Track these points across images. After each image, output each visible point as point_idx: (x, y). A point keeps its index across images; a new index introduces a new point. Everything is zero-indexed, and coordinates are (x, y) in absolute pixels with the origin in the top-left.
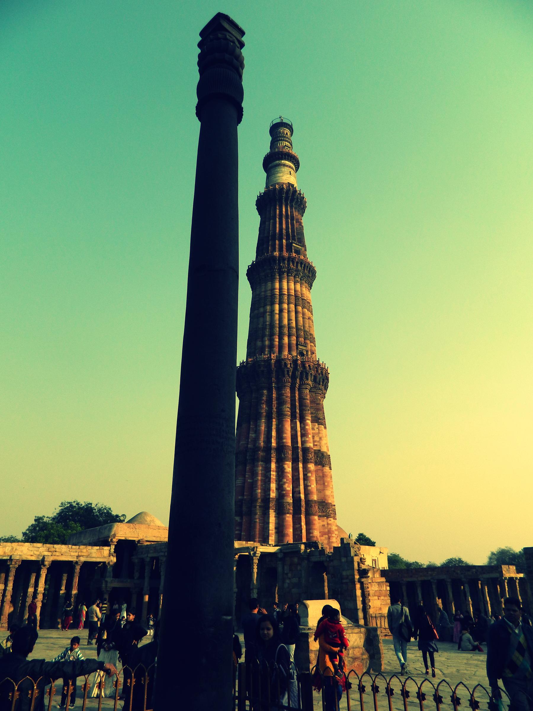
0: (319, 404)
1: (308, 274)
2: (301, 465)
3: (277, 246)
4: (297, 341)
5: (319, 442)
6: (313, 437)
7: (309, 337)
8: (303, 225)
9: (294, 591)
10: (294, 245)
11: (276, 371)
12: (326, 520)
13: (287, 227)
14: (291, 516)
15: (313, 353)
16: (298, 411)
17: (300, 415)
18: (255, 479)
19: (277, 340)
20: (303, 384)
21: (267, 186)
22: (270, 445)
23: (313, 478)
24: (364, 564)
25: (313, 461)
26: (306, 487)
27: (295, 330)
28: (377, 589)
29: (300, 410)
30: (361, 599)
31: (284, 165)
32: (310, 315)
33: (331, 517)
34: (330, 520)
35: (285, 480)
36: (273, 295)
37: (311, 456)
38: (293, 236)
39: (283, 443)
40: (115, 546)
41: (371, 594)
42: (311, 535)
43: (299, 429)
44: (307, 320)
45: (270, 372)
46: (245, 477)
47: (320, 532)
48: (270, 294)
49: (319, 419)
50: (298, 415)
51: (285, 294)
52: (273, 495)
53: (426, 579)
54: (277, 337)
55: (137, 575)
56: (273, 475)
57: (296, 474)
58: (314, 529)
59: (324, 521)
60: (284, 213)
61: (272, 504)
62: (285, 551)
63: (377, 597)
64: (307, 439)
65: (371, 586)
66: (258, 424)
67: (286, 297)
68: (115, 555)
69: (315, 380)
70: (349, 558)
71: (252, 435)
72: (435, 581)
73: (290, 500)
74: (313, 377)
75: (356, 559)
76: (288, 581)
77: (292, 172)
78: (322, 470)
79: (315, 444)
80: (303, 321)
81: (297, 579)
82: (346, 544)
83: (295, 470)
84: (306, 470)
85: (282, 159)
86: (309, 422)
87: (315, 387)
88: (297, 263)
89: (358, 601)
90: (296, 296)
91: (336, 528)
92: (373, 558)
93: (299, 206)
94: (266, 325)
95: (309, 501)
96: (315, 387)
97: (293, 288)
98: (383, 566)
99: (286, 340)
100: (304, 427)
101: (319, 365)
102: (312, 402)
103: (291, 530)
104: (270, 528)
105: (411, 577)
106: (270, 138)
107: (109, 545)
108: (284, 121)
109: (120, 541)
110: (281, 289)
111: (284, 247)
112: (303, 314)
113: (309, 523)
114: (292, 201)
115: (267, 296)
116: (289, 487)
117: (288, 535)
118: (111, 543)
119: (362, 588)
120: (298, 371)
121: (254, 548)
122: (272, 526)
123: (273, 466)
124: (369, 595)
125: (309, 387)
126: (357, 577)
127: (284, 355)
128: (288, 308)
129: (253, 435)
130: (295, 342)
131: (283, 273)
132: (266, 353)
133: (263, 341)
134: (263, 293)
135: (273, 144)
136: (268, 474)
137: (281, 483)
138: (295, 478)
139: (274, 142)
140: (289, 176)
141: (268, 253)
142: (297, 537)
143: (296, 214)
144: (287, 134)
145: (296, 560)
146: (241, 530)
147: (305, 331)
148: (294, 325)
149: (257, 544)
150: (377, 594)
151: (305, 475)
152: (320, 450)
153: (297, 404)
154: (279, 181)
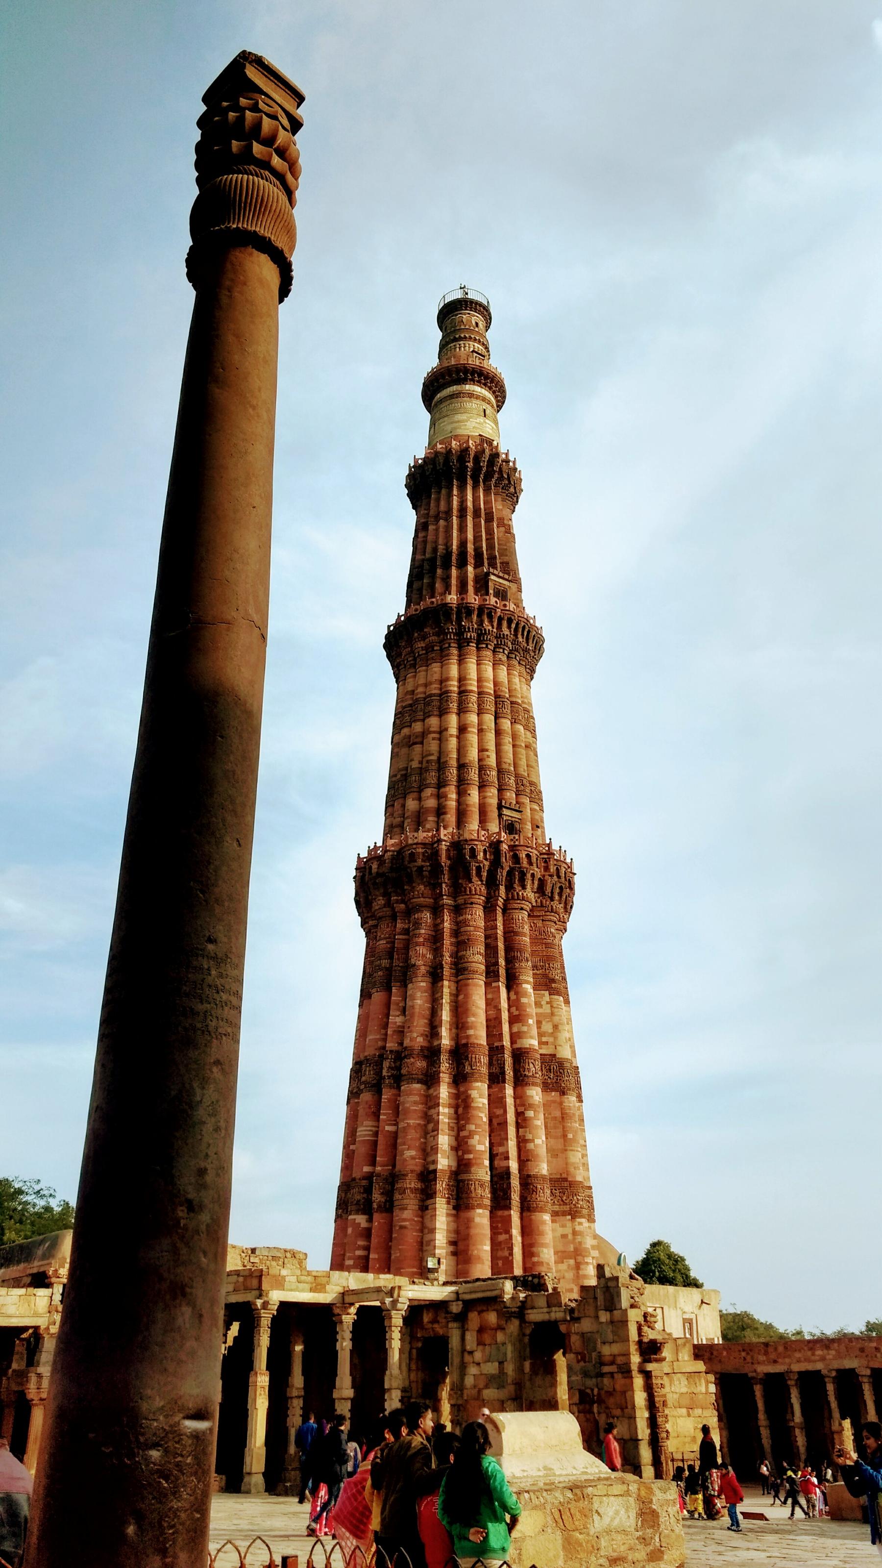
0: (548, 946)
1: (523, 644)
2: (509, 1091)
3: (454, 581)
4: (500, 800)
5: (552, 1034)
6: (539, 1023)
7: (529, 789)
8: (516, 530)
9: (489, 1393)
11: (451, 868)
12: (569, 1224)
13: (477, 538)
14: (487, 1213)
15: (537, 826)
16: (502, 962)
17: (507, 970)
18: (401, 1125)
19: (454, 796)
20: (513, 898)
21: (431, 445)
22: (436, 1043)
23: (539, 1122)
25: (538, 1081)
26: (522, 1142)
27: (494, 773)
28: (684, 1390)
30: (647, 1415)
31: (471, 395)
32: (531, 740)
34: (580, 1224)
35: (473, 1127)
36: (444, 694)
37: (534, 1068)
39: (468, 1037)
40: (64, 1285)
41: (670, 1403)
42: (535, 1259)
43: (504, 1004)
44: (523, 751)
45: (436, 869)
46: (378, 1120)
47: (556, 1253)
48: (437, 692)
49: (553, 981)
50: (502, 972)
51: (471, 691)
52: (444, 1162)
53: (810, 1367)
56: (444, 1114)
57: (499, 1112)
58: (543, 1245)
59: (566, 1226)
60: (470, 504)
61: (441, 1186)
62: (467, 1297)
63: (684, 1411)
64: (525, 1029)
65: (671, 1382)
67: (474, 698)
69: (541, 890)
71: (396, 1019)
72: (834, 1374)
73: (482, 1173)
74: (536, 883)
75: (634, 1316)
76: (473, 1370)
78: (561, 1103)
79: (544, 1039)
80: (515, 754)
81: (497, 1364)
82: (610, 1279)
83: (496, 1102)
85: (464, 381)
87: (542, 906)
88: (500, 619)
89: (638, 1420)
90: (497, 696)
91: (594, 1242)
92: (687, 1316)
93: (506, 487)
94: (428, 762)
95: (529, 1176)
96: (542, 906)
97: (492, 678)
99: (474, 796)
100: (518, 1000)
101: (550, 853)
102: (534, 940)
103: (487, 1248)
104: (437, 1243)
105: (775, 1362)
106: (438, 335)
107: (48, 1285)
110: (462, 679)
111: (471, 584)
112: (514, 737)
113: (527, 1230)
114: (488, 476)
115: (431, 695)
116: (481, 1144)
117: (479, 1258)
118: (53, 1280)
119: (649, 1388)
120: (502, 868)
121: (393, 1289)
122: (441, 1239)
123: (444, 1092)
124: (665, 1404)
125: (527, 906)
126: (635, 1359)
128: (480, 723)
130: (493, 801)
131: (468, 641)
132: (428, 826)
133: (420, 799)
134: (421, 689)
135: (443, 346)
136: (432, 1111)
137: (463, 1134)
138: (495, 1122)
139: (447, 343)
140: (481, 419)
141: (433, 596)
142: (500, 1263)
143: (498, 506)
144: (477, 324)
145: (492, 1318)
146: (367, 1248)
147: (517, 776)
148: (492, 761)
150: (686, 1401)
151: (519, 1114)
152: (555, 1055)
153: (501, 945)
154: (461, 432)
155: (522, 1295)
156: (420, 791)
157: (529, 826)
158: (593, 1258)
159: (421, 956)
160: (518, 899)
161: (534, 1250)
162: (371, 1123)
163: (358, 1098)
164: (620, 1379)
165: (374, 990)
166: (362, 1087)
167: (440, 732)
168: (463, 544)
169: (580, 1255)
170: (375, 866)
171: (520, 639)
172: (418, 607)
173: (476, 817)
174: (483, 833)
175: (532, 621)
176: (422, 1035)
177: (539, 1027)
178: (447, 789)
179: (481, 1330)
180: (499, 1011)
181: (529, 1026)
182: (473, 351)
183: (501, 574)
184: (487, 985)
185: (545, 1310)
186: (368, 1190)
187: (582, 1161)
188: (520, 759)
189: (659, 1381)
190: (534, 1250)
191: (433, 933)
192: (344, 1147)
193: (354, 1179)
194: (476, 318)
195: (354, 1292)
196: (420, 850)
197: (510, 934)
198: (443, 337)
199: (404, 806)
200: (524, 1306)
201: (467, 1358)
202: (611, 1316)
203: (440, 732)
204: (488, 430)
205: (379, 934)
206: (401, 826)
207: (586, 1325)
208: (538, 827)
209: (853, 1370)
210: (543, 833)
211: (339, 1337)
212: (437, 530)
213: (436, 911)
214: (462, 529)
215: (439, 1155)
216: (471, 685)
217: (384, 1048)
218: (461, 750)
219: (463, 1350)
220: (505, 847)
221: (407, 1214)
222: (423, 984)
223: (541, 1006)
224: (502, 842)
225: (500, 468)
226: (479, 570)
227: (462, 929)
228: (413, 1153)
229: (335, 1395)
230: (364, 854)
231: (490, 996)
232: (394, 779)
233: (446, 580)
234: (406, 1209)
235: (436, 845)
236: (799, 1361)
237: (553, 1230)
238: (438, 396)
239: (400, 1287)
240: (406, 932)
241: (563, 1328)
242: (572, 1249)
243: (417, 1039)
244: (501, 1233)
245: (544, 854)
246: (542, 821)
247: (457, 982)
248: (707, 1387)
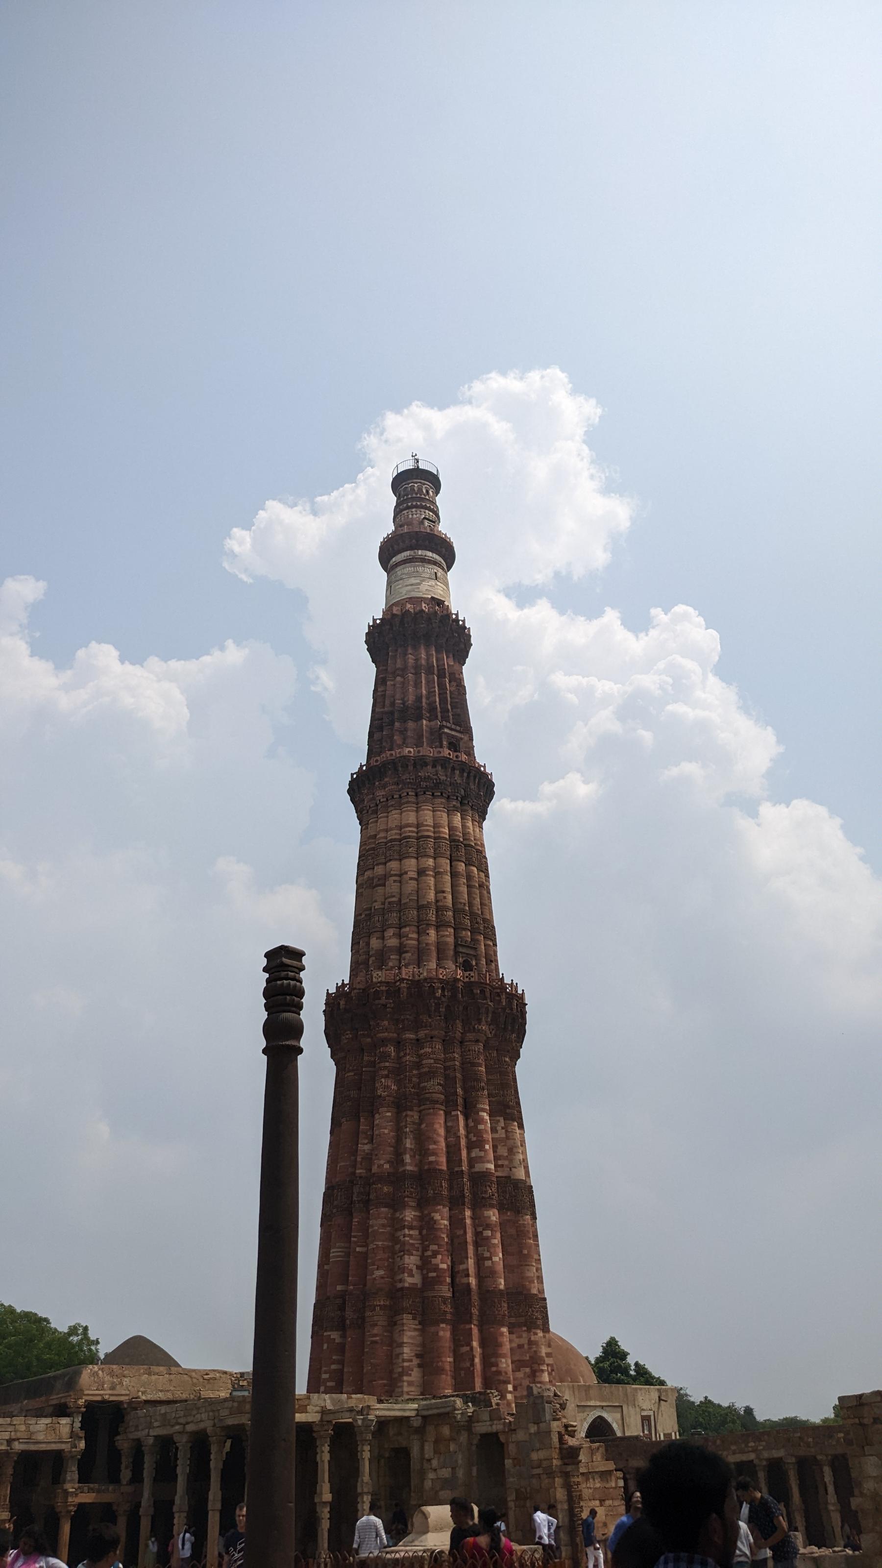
2: (468, 1213)
3: (409, 733)
5: (506, 1158)
6: (495, 1147)
8: (467, 683)
10: (446, 730)
12: (525, 1335)
13: (430, 693)
15: (492, 960)
17: (465, 1100)
18: (371, 1246)
19: (415, 936)
24: (572, 1434)
26: (480, 1260)
27: (450, 913)
28: (598, 1485)
29: (464, 1089)
30: (566, 1507)
33: (537, 1328)
38: (445, 711)
40: (83, 1414)
42: (494, 1369)
43: (462, 1131)
48: (398, 837)
49: (508, 1107)
51: (429, 837)
53: (744, 1458)
54: (415, 929)
55: (126, 1474)
56: (410, 1236)
60: (423, 662)
62: (425, 1413)
64: (482, 1154)
65: (587, 1480)
66: (377, 1122)
68: (82, 1434)
70: (542, 1425)
71: (365, 1147)
72: (764, 1463)
73: (446, 1291)
74: (490, 1015)
75: (556, 1426)
76: (431, 1475)
77: (440, 573)
79: (500, 1163)
80: (469, 894)
82: (536, 1397)
83: (456, 1222)
84: (480, 1223)
86: (486, 1116)
87: (495, 1035)
90: (453, 840)
92: (644, 1413)
94: (389, 903)
95: (488, 1291)
98: (669, 1432)
104: (405, 1356)
108: (422, 466)
109: (90, 1405)
112: (469, 877)
115: (391, 841)
117: (442, 1370)
119: (568, 1487)
123: (409, 1215)
124: (580, 1498)
127: (429, 971)
129: (367, 1148)
130: (451, 940)
132: (391, 964)
133: (383, 938)
135: (398, 511)
136: (399, 1233)
140: (433, 582)
142: (462, 1372)
144: (427, 492)
145: (446, 1431)
146: (341, 1362)
149: (371, 1401)
151: (477, 1234)
153: (458, 1075)
155: (471, 1410)
156: (383, 931)
157: (483, 961)
158: (548, 1365)
159: (386, 1086)
160: (474, 1032)
161: (493, 1360)
162: (343, 1245)
163: (331, 1221)
164: (546, 1482)
165: (344, 1120)
166: (334, 1211)
167: (400, 875)
168: (419, 698)
169: (537, 1363)
170: (342, 1002)
171: (473, 787)
172: (378, 758)
173: (434, 954)
174: (441, 971)
175: (482, 769)
176: (388, 1162)
177: (495, 1152)
178: (407, 929)
179: (436, 1442)
180: (458, 1138)
181: (486, 1151)
182: (425, 518)
183: (453, 727)
184: (447, 1114)
185: (488, 1423)
186: (342, 1308)
187: (536, 1274)
188: (474, 899)
189: (576, 1480)
190: (493, 1360)
191: (398, 1066)
192: (320, 1266)
193: (328, 1298)
194: (426, 486)
195: (330, 1412)
196: (384, 988)
197: (468, 1066)
198: (398, 504)
199: (368, 944)
200: (471, 1420)
201: (426, 1465)
202: (538, 1428)
203: (400, 875)
204: (438, 592)
205: (348, 1066)
206: (366, 963)
207: (521, 1436)
208: (492, 961)
209: (781, 1458)
210: (497, 966)
211: (318, 1450)
212: (394, 685)
213: (399, 1044)
214: (417, 684)
215: (406, 1275)
216: (428, 831)
217: (354, 1173)
218: (420, 892)
219: (422, 1458)
220: (460, 985)
221: (376, 1331)
222: (389, 1114)
223: (497, 1132)
224: (459, 980)
225: (451, 629)
226: (433, 723)
227: (424, 1062)
228: (382, 1272)
229: (316, 1500)
230: (333, 990)
231: (449, 1124)
232: (359, 918)
233: (403, 732)
234: (376, 1325)
235: (398, 984)
236: (734, 1453)
237: (511, 1341)
238: (394, 559)
239: (369, 1407)
240: (373, 1064)
241: (502, 1438)
242: (528, 1358)
243: (383, 1164)
244: (463, 1346)
245: (497, 988)
246: (496, 955)
247: (420, 1112)
248: (616, 1482)
